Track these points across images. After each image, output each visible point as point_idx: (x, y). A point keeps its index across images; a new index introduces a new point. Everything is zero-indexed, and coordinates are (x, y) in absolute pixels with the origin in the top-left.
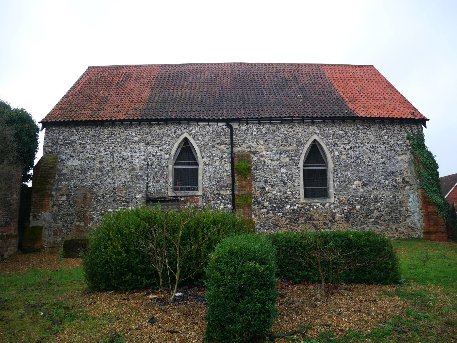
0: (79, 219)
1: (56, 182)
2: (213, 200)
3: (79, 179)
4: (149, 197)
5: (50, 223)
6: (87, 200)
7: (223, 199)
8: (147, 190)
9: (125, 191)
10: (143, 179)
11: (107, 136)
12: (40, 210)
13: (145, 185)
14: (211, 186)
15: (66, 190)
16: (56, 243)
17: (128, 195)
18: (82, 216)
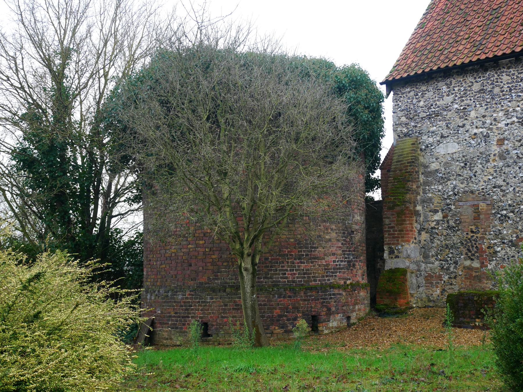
0: (470, 254)
1: (422, 187)
3: (461, 178)
5: (417, 263)
6: (482, 217)
11: (508, 87)
12: (400, 239)
15: (440, 201)
16: (432, 299)
18: (475, 250)
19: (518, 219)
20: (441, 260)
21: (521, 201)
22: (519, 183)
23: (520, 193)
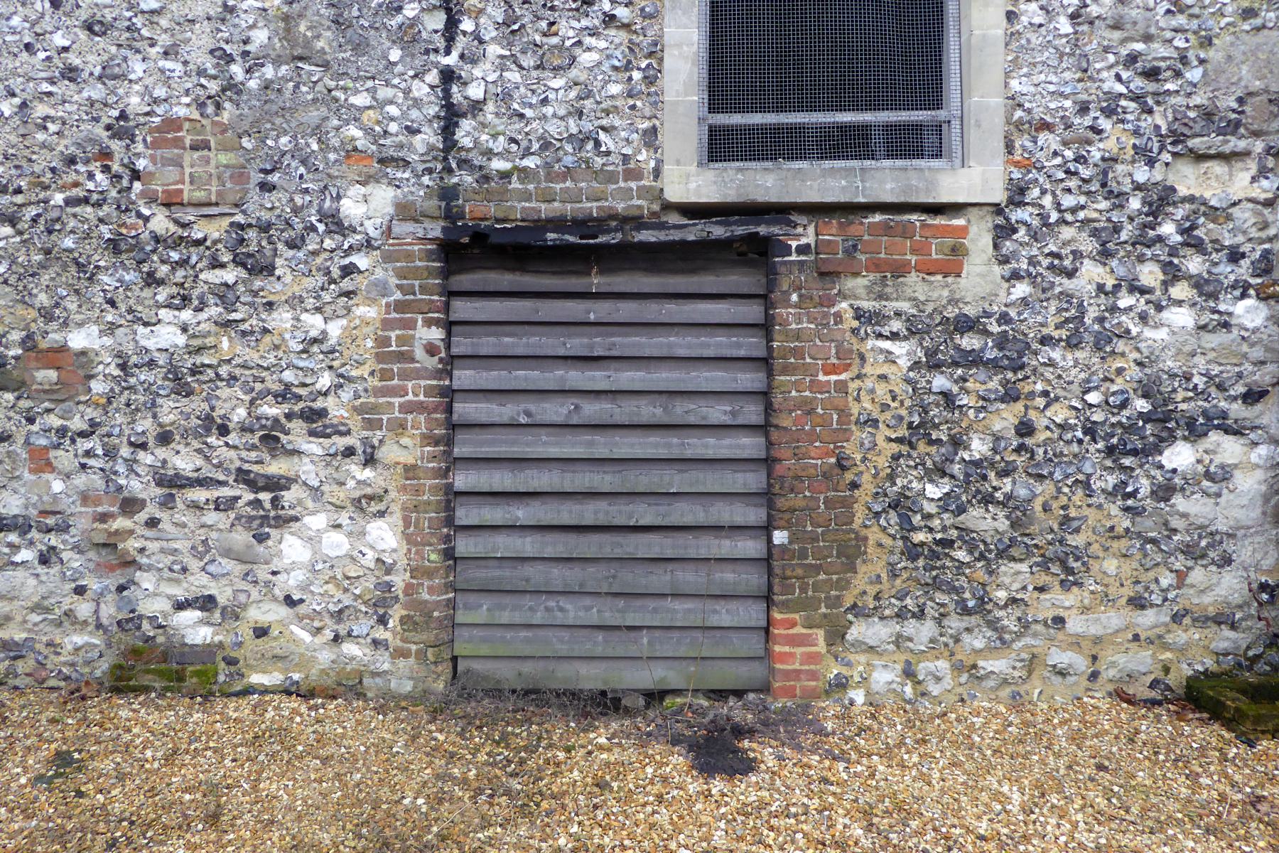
2: (1105, 255)
4: (476, 209)
7: (1198, 246)
8: (450, 144)
9: (225, 148)
10: (408, 36)
13: (420, 90)
14: (1084, 109)
17: (254, 195)
19: (38, 258)
21: (53, 170)
22: (52, 81)
23: (52, 127)
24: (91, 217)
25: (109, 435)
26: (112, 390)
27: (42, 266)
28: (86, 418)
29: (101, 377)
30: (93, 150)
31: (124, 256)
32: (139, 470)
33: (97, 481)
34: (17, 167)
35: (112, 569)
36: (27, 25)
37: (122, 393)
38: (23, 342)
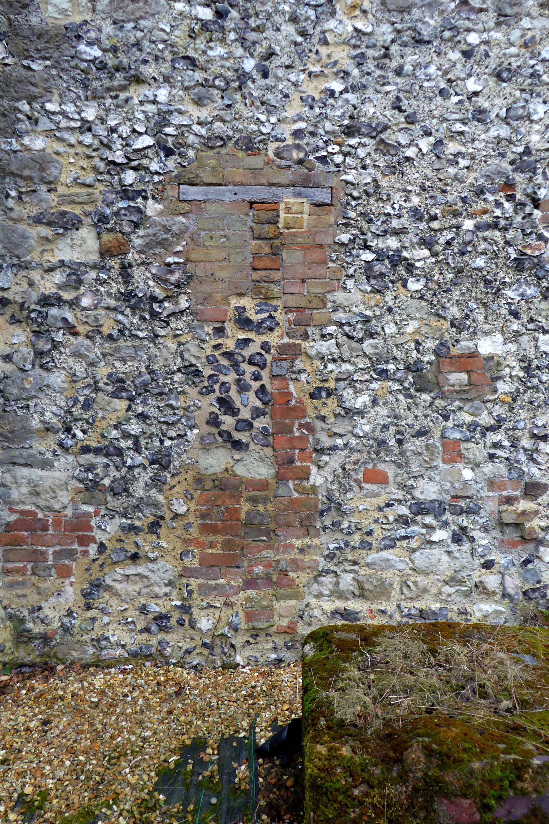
0: (228, 422)
3: (199, 76)
15: (89, 178)
16: (37, 629)
20: (86, 450)
21: (464, 200)
23: (463, 163)
24: (499, 239)
25: (514, 429)
26: (518, 390)
27: (454, 283)
28: (494, 414)
29: (507, 379)
30: (499, 181)
31: (526, 274)
32: (539, 460)
33: (501, 468)
34: (431, 197)
35: (514, 545)
36: (440, 73)
37: (525, 392)
38: (436, 352)
